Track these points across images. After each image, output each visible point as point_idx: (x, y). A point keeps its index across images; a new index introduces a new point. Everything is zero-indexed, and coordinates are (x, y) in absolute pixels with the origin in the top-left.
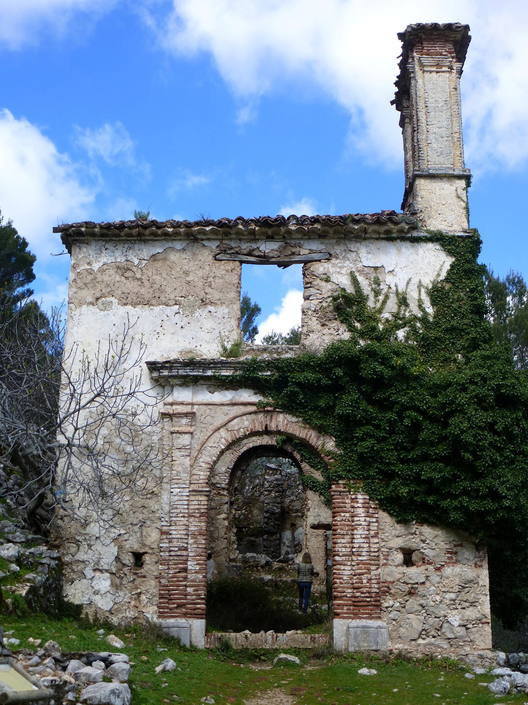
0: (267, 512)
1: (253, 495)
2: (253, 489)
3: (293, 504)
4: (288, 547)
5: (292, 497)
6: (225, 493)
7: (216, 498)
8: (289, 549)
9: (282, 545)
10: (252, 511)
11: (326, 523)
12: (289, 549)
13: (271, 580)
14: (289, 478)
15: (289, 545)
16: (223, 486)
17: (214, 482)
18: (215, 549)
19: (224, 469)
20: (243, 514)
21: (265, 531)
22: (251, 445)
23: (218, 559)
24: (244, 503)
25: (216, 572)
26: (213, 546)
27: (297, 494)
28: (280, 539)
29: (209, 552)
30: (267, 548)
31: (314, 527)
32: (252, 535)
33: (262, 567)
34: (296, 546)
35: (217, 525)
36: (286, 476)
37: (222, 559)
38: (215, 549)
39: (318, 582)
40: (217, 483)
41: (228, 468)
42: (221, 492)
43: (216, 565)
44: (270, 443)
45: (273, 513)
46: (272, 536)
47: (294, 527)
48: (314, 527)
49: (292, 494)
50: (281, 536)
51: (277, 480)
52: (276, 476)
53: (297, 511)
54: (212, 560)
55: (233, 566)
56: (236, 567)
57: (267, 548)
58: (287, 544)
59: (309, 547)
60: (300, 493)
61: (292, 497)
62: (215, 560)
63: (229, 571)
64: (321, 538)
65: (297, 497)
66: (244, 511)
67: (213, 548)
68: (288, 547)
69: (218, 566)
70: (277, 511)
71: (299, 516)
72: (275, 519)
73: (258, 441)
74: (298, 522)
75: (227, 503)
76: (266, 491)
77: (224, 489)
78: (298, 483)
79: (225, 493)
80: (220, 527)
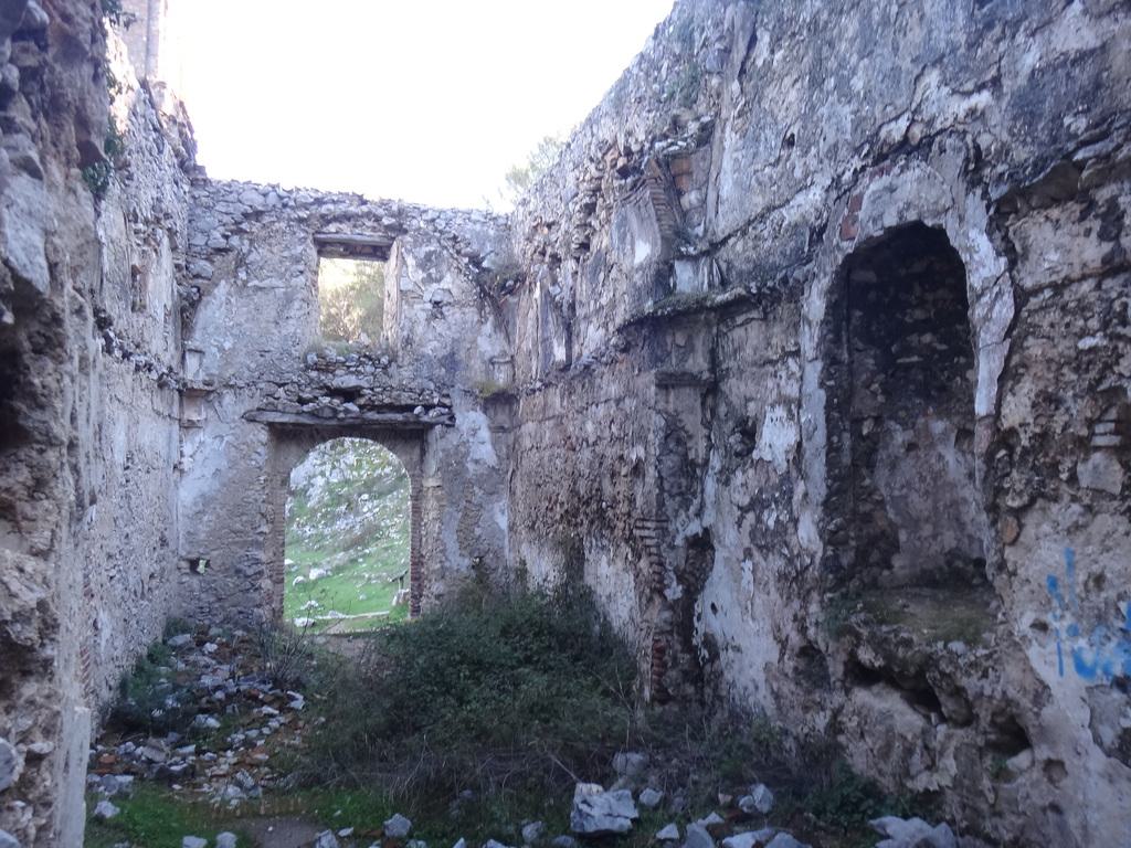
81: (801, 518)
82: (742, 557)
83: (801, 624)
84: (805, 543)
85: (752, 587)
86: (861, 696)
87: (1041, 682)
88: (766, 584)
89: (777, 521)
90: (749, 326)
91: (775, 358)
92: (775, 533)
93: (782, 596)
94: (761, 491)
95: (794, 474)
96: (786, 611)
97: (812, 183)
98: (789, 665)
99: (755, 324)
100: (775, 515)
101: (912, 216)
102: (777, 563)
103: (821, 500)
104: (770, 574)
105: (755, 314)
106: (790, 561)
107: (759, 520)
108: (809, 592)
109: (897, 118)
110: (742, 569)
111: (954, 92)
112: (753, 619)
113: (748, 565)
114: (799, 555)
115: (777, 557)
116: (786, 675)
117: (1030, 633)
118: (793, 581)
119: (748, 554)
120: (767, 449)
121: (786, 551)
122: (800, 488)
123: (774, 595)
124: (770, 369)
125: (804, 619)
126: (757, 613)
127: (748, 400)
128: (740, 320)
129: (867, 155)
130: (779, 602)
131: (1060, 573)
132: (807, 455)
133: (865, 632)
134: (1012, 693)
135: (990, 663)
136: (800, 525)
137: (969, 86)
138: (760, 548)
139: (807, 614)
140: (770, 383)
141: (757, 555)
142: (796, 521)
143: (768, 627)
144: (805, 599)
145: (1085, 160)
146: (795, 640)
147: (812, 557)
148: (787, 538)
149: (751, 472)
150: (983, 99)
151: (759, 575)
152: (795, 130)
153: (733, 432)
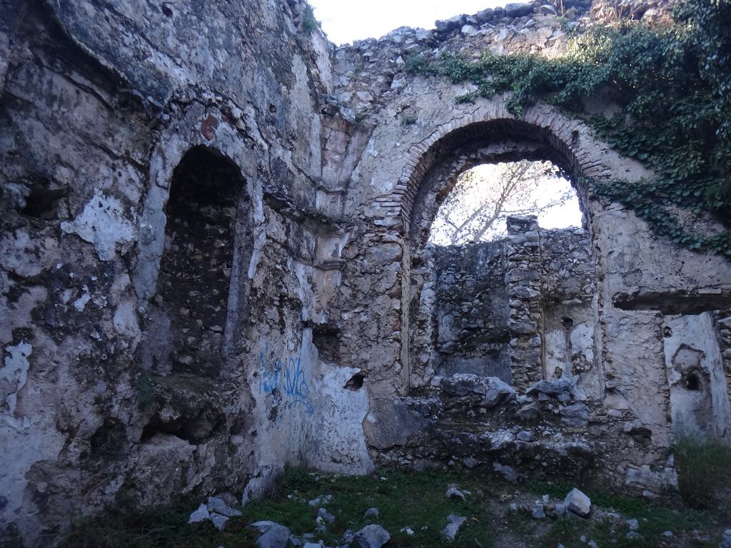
0: (514, 297)
1: (491, 273)
2: (491, 263)
3: (565, 284)
4: (560, 360)
5: (562, 272)
6: (393, 236)
7: (374, 250)
8: (562, 365)
9: (548, 356)
10: (490, 301)
11: (661, 291)
12: (562, 365)
13: (510, 446)
14: (555, 241)
15: (561, 356)
16: (389, 222)
17: (369, 214)
18: (370, 366)
19: (390, 186)
20: (477, 306)
21: (513, 332)
22: (449, 128)
23: (377, 389)
24: (477, 289)
25: (371, 418)
26: (365, 356)
27: (570, 266)
28: (543, 344)
29: (358, 370)
30: (518, 362)
31: (624, 302)
32: (490, 341)
33: (492, 408)
34: (574, 358)
35: (376, 309)
36: (548, 237)
37: (386, 388)
38: (370, 366)
39: (650, 457)
40: (375, 217)
41: (400, 183)
42: (387, 236)
43: (373, 403)
44: (493, 116)
45: (526, 300)
46: (526, 340)
47: (568, 323)
48: (624, 302)
49: (562, 266)
50: (543, 341)
51: (530, 240)
52: (527, 233)
53: (573, 296)
54: (362, 391)
55: (412, 407)
56: (419, 408)
57: (518, 362)
58: (557, 354)
59: (613, 357)
60: (576, 265)
61: (562, 272)
62: (370, 391)
63: (403, 417)
64: (646, 334)
65: (570, 271)
66: (476, 301)
67: (366, 362)
68: (560, 360)
69: (377, 405)
70: (533, 295)
71: (577, 305)
72: (530, 309)
73: (466, 117)
74: (576, 315)
75: (399, 259)
76: (511, 260)
77: (391, 228)
78: (571, 247)
79: (393, 236)
80: (382, 313)
81: (120, 307)
82: (9, 338)
83: (102, 404)
84: (121, 330)
85: (23, 377)
86: (152, 449)
87: (253, 399)
88: (54, 370)
89: (90, 305)
90: (83, 94)
91: (115, 152)
92: (81, 316)
93: (79, 381)
94: (67, 268)
95: (119, 265)
96: (83, 396)
97: (180, 66)
98: (75, 451)
99: (93, 99)
100: (86, 298)
101: (238, 163)
102: (79, 346)
103: (149, 295)
104: (63, 360)
105: (105, 97)
106: (99, 345)
107: (54, 297)
108: (119, 373)
109: (237, 106)
110: (10, 354)
111: (259, 129)
112: (18, 415)
113: (26, 348)
114: (114, 340)
115: (80, 340)
116: (70, 465)
117: (253, 378)
118: (104, 363)
119: (21, 335)
120: (89, 230)
121: (97, 336)
122: (124, 280)
123: (66, 380)
124: (107, 157)
125: (110, 399)
126: (28, 406)
127: (59, 161)
128: (76, 77)
129: (218, 101)
130: (75, 387)
131: (263, 351)
132: (141, 255)
133: (169, 398)
134: (243, 407)
135: (235, 396)
136: (118, 314)
137: (264, 135)
138: (50, 330)
139: (116, 393)
140: (104, 170)
141: (42, 338)
142: (113, 308)
143: (49, 416)
144: (112, 380)
145: (288, 206)
146: (92, 420)
147: (130, 341)
148: (101, 323)
149: (50, 242)
150: (266, 147)
151: (41, 360)
152: (175, 13)
153: (18, 180)
